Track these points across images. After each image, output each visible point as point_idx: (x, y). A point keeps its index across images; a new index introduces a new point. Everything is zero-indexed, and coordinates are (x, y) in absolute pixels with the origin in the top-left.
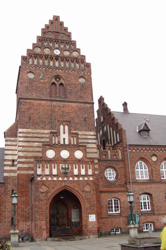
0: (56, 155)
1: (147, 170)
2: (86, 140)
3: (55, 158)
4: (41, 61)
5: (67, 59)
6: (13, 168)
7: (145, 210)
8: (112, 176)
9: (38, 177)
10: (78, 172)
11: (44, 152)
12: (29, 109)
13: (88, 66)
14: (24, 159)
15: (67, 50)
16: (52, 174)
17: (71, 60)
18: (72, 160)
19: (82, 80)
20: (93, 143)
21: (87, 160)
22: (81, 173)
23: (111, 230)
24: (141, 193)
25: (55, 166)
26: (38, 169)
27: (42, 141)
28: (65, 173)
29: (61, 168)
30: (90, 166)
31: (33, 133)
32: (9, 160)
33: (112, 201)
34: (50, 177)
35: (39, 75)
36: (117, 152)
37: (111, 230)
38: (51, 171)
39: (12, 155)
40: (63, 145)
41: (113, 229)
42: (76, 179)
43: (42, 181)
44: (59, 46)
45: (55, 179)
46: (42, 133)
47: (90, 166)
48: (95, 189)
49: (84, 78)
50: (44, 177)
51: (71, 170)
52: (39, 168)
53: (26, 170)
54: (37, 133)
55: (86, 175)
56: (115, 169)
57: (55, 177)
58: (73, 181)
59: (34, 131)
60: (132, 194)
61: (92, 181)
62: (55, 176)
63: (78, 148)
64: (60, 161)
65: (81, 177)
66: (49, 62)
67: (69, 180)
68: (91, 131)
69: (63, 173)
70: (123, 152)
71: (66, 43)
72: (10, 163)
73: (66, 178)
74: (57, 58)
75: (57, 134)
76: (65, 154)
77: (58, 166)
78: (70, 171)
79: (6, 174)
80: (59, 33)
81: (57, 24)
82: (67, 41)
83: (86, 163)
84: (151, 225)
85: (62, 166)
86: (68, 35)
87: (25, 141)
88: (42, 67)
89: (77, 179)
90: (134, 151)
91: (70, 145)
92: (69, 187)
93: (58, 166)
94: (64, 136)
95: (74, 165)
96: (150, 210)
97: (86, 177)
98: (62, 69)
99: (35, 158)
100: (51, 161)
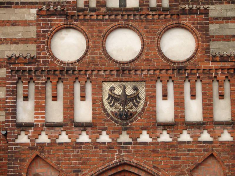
0: (88, 48)
3: (86, 59)
9: (19, 134)
10: (176, 111)
11: (44, 39)
16: (73, 121)
18: (152, 67)
21: (211, 65)
22: (183, 117)
25: (83, 89)
26: (21, 102)
28: (125, 118)
29: (106, 96)
30: (221, 86)
34: (64, 133)
38: (69, 108)
40: (115, 10)
42: (165, 137)
43: (36, 148)
45: (84, 138)
47: (221, 86)
50: (43, 133)
51: (146, 104)
52: (26, 98)
55: (208, 123)
57: (84, 133)
58: (155, 147)
62: (84, 127)
63: (173, 20)
64: (102, 73)
65: (185, 132)
67: (139, 140)
69: (116, 115)
73: (124, 133)
76: (124, 45)
77: (98, 91)
78: (143, 109)
83: (208, 77)
85: (112, 89)
89: (170, 140)
91: (145, 11)
92: (136, 167)
93: (98, 91)
95: (159, 87)
97: (206, 132)
99: (11, 63)
100: (70, 72)
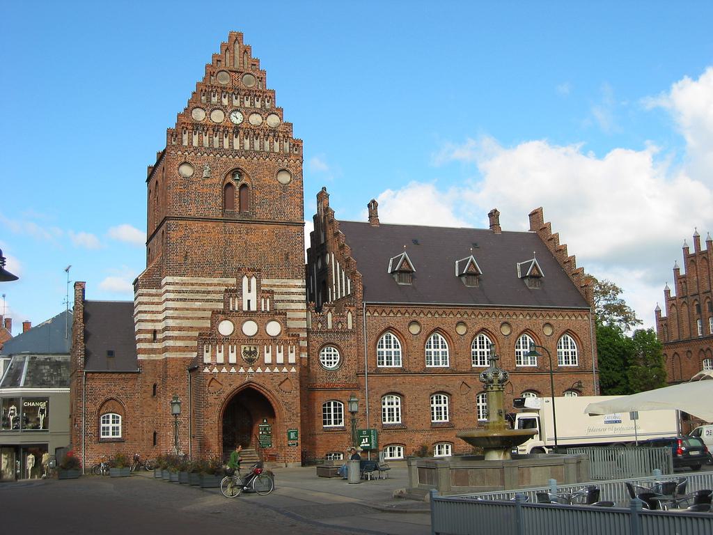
0: (234, 329)
1: (400, 350)
2: (288, 296)
4: (206, 139)
5: (256, 132)
6: (155, 346)
7: (391, 422)
8: (333, 360)
12: (185, 237)
13: (297, 145)
14: (178, 332)
15: (256, 113)
17: (264, 135)
18: (263, 339)
19: (284, 178)
20: (299, 301)
23: (327, 455)
24: (384, 393)
25: (232, 348)
27: (208, 297)
31: (192, 284)
32: (147, 331)
33: (329, 405)
35: (202, 170)
36: (343, 316)
37: (327, 455)
38: (226, 357)
39: (153, 321)
41: (331, 455)
42: (268, 370)
44: (242, 102)
46: (208, 284)
48: (299, 388)
49: (288, 171)
52: (207, 352)
53: (180, 351)
54: (200, 285)
55: (286, 364)
56: (338, 347)
58: (263, 375)
59: (194, 280)
60: (356, 399)
61: (295, 374)
66: (221, 141)
68: (296, 278)
70: (357, 317)
71: (255, 95)
72: (149, 336)
74: (236, 130)
75: (235, 292)
76: (250, 328)
79: (140, 357)
80: (242, 72)
81: (237, 53)
82: (256, 91)
83: (286, 343)
84: (399, 450)
85: (245, 348)
86: (258, 78)
87: (178, 300)
88: (208, 151)
90: (376, 314)
94: (249, 297)
96: (400, 422)
98: (246, 154)
